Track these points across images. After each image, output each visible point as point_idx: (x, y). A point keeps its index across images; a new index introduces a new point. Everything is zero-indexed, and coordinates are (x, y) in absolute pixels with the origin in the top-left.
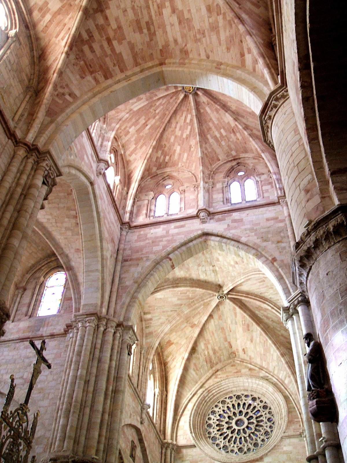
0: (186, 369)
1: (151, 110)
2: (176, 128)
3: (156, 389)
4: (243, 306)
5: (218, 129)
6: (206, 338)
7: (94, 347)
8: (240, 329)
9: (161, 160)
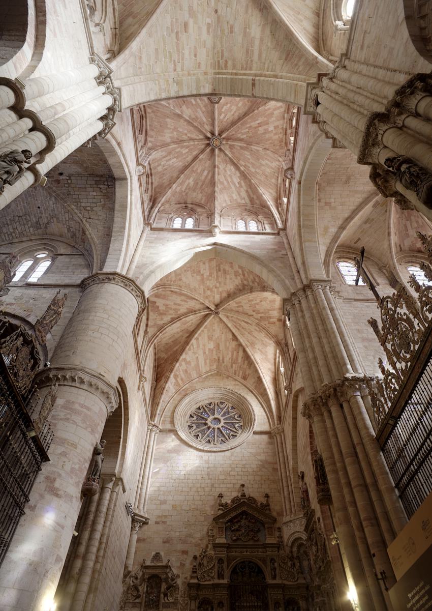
1: (251, 134)
5: (197, 105)
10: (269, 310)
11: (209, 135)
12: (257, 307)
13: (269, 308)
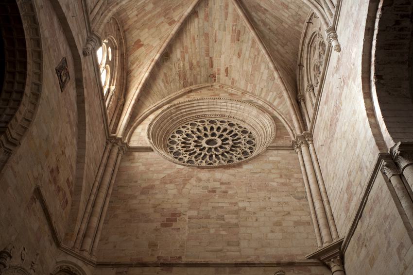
0: (153, 76)
3: (111, 87)
6: (185, 44)
8: (228, 38)
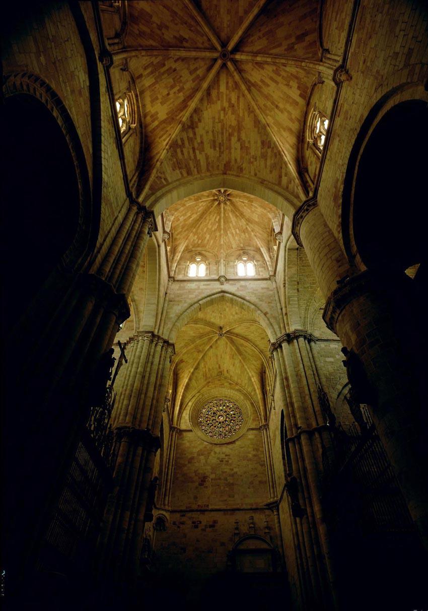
1: (196, 208)
2: (208, 223)
4: (232, 342)
5: (235, 228)
7: (149, 354)
8: (228, 357)
9: (196, 242)
10: (156, 82)
11: (228, 203)
12: (171, 80)
13: (157, 86)
